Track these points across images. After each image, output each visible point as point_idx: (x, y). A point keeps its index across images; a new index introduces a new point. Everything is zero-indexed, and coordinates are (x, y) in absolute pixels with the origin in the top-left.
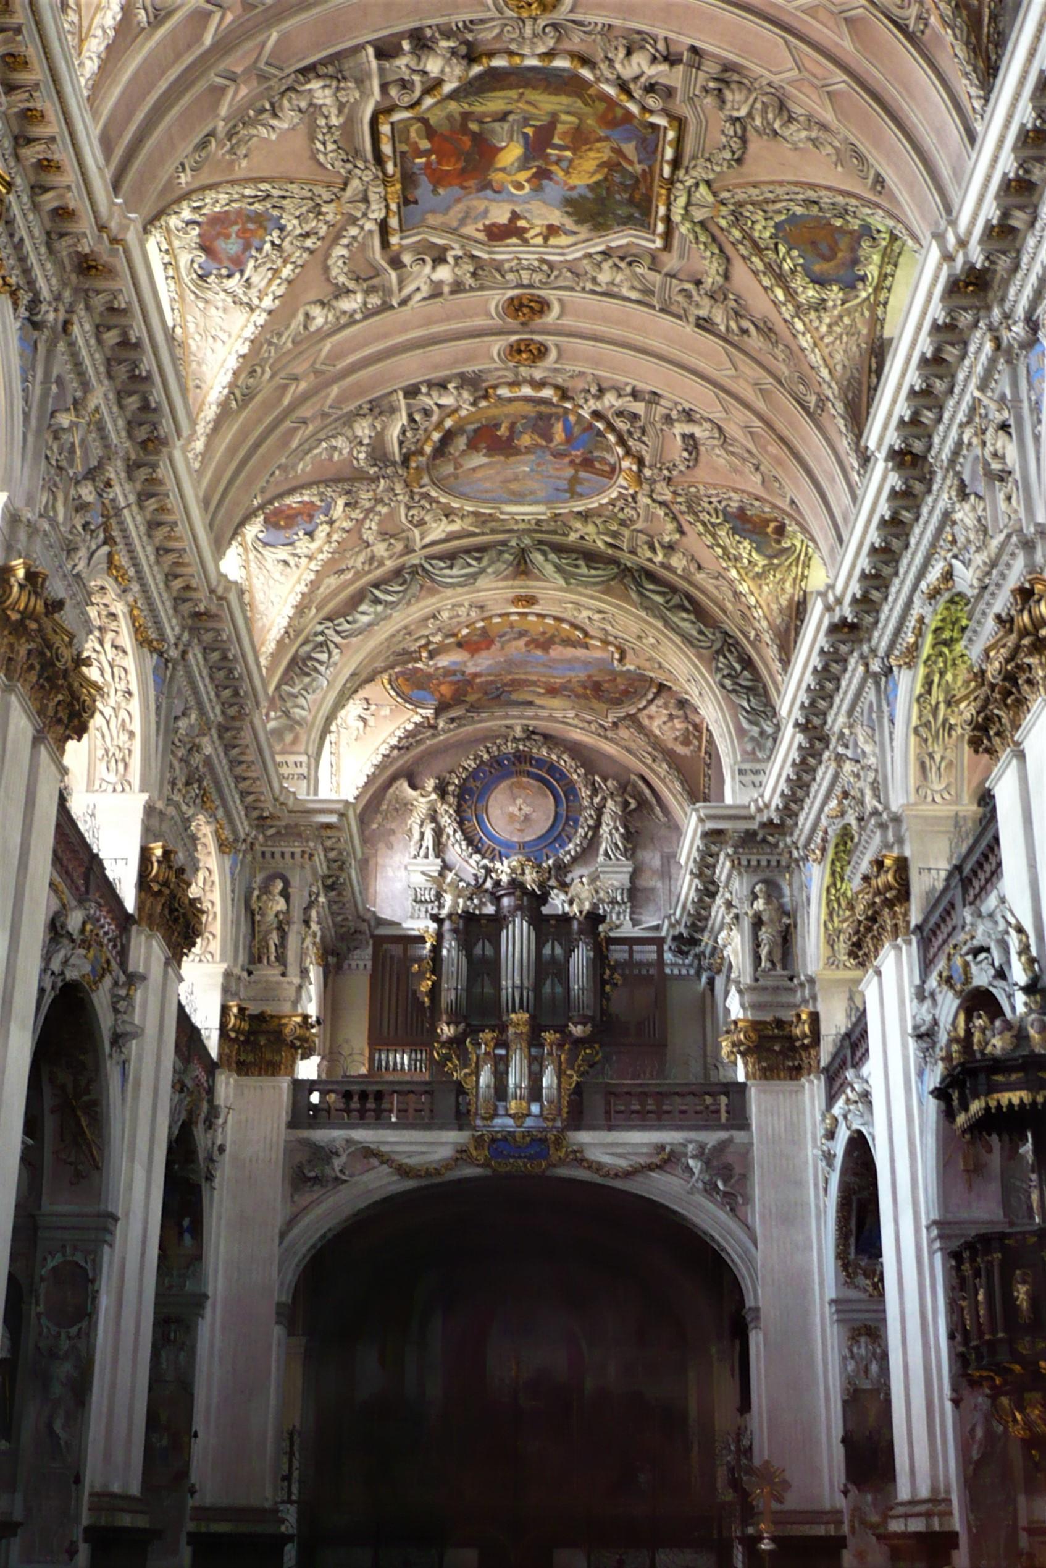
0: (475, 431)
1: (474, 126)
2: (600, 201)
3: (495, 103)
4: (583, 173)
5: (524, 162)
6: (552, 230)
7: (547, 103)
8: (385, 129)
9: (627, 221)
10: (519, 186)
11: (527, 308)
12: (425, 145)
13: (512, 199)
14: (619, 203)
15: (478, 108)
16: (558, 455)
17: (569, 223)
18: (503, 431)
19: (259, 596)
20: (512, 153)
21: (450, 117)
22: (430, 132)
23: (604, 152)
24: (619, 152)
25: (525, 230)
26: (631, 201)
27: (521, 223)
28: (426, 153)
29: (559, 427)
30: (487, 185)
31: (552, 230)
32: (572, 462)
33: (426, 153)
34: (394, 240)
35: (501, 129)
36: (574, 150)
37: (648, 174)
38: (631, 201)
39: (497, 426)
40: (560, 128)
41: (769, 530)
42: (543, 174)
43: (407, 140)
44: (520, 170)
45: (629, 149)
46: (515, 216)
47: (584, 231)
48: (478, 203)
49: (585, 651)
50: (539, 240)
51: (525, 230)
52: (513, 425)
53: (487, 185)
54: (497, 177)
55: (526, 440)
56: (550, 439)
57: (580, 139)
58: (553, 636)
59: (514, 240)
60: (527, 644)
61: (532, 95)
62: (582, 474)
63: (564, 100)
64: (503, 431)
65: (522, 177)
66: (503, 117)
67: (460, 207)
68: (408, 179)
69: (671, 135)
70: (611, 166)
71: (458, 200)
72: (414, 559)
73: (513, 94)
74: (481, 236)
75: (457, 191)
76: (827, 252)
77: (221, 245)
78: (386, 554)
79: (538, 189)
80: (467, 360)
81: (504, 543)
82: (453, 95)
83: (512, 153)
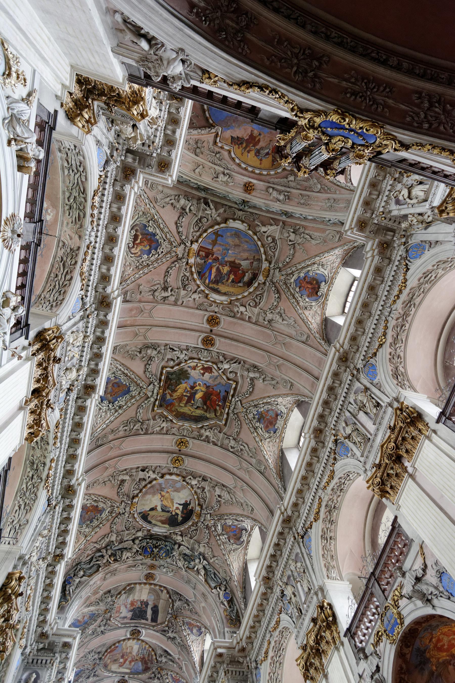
0: (240, 282)
1: (205, 407)
2: (179, 379)
3: (199, 412)
4: (183, 387)
5: (195, 393)
6: (194, 368)
7: (186, 410)
8: (224, 422)
9: (172, 374)
10: (199, 384)
11: (208, 342)
12: (218, 408)
13: (202, 381)
14: (174, 379)
15: (203, 412)
16: (217, 259)
17: (189, 370)
18: (232, 277)
19: (339, 260)
20: (199, 396)
21: (210, 413)
22: (215, 411)
23: (175, 395)
24: (171, 396)
25: (202, 369)
26: (171, 380)
27: (202, 372)
28: (219, 405)
29: (213, 277)
30: (208, 387)
31: (194, 368)
32: (213, 255)
33: (219, 405)
34: (234, 386)
35: (199, 404)
36: (183, 395)
37: (164, 391)
38: (171, 380)
39: (233, 281)
40: (185, 402)
41: (140, 237)
42: (192, 388)
43: (221, 412)
44: (197, 390)
45: (168, 397)
46: (203, 374)
47: (186, 368)
48: (211, 382)
49: (235, 135)
50: (199, 365)
51: (202, 369)
52: (227, 280)
53: (208, 387)
54: (204, 389)
55: (226, 269)
56: (218, 269)
57: (180, 399)
58: (245, 148)
59: (206, 366)
60: (259, 141)
61: (189, 412)
62: (210, 247)
63: (182, 410)
64: (232, 277)
65: (198, 388)
66: (198, 408)
67: (216, 383)
68: (225, 399)
69: (156, 409)
70: (174, 391)
71: (216, 385)
72: (284, 218)
73: (194, 414)
74: (214, 370)
75: (215, 388)
76: (115, 385)
77: (274, 416)
78: (291, 234)
79: (195, 383)
80: (231, 323)
81: (250, 207)
82: (207, 419)
83: (199, 396)
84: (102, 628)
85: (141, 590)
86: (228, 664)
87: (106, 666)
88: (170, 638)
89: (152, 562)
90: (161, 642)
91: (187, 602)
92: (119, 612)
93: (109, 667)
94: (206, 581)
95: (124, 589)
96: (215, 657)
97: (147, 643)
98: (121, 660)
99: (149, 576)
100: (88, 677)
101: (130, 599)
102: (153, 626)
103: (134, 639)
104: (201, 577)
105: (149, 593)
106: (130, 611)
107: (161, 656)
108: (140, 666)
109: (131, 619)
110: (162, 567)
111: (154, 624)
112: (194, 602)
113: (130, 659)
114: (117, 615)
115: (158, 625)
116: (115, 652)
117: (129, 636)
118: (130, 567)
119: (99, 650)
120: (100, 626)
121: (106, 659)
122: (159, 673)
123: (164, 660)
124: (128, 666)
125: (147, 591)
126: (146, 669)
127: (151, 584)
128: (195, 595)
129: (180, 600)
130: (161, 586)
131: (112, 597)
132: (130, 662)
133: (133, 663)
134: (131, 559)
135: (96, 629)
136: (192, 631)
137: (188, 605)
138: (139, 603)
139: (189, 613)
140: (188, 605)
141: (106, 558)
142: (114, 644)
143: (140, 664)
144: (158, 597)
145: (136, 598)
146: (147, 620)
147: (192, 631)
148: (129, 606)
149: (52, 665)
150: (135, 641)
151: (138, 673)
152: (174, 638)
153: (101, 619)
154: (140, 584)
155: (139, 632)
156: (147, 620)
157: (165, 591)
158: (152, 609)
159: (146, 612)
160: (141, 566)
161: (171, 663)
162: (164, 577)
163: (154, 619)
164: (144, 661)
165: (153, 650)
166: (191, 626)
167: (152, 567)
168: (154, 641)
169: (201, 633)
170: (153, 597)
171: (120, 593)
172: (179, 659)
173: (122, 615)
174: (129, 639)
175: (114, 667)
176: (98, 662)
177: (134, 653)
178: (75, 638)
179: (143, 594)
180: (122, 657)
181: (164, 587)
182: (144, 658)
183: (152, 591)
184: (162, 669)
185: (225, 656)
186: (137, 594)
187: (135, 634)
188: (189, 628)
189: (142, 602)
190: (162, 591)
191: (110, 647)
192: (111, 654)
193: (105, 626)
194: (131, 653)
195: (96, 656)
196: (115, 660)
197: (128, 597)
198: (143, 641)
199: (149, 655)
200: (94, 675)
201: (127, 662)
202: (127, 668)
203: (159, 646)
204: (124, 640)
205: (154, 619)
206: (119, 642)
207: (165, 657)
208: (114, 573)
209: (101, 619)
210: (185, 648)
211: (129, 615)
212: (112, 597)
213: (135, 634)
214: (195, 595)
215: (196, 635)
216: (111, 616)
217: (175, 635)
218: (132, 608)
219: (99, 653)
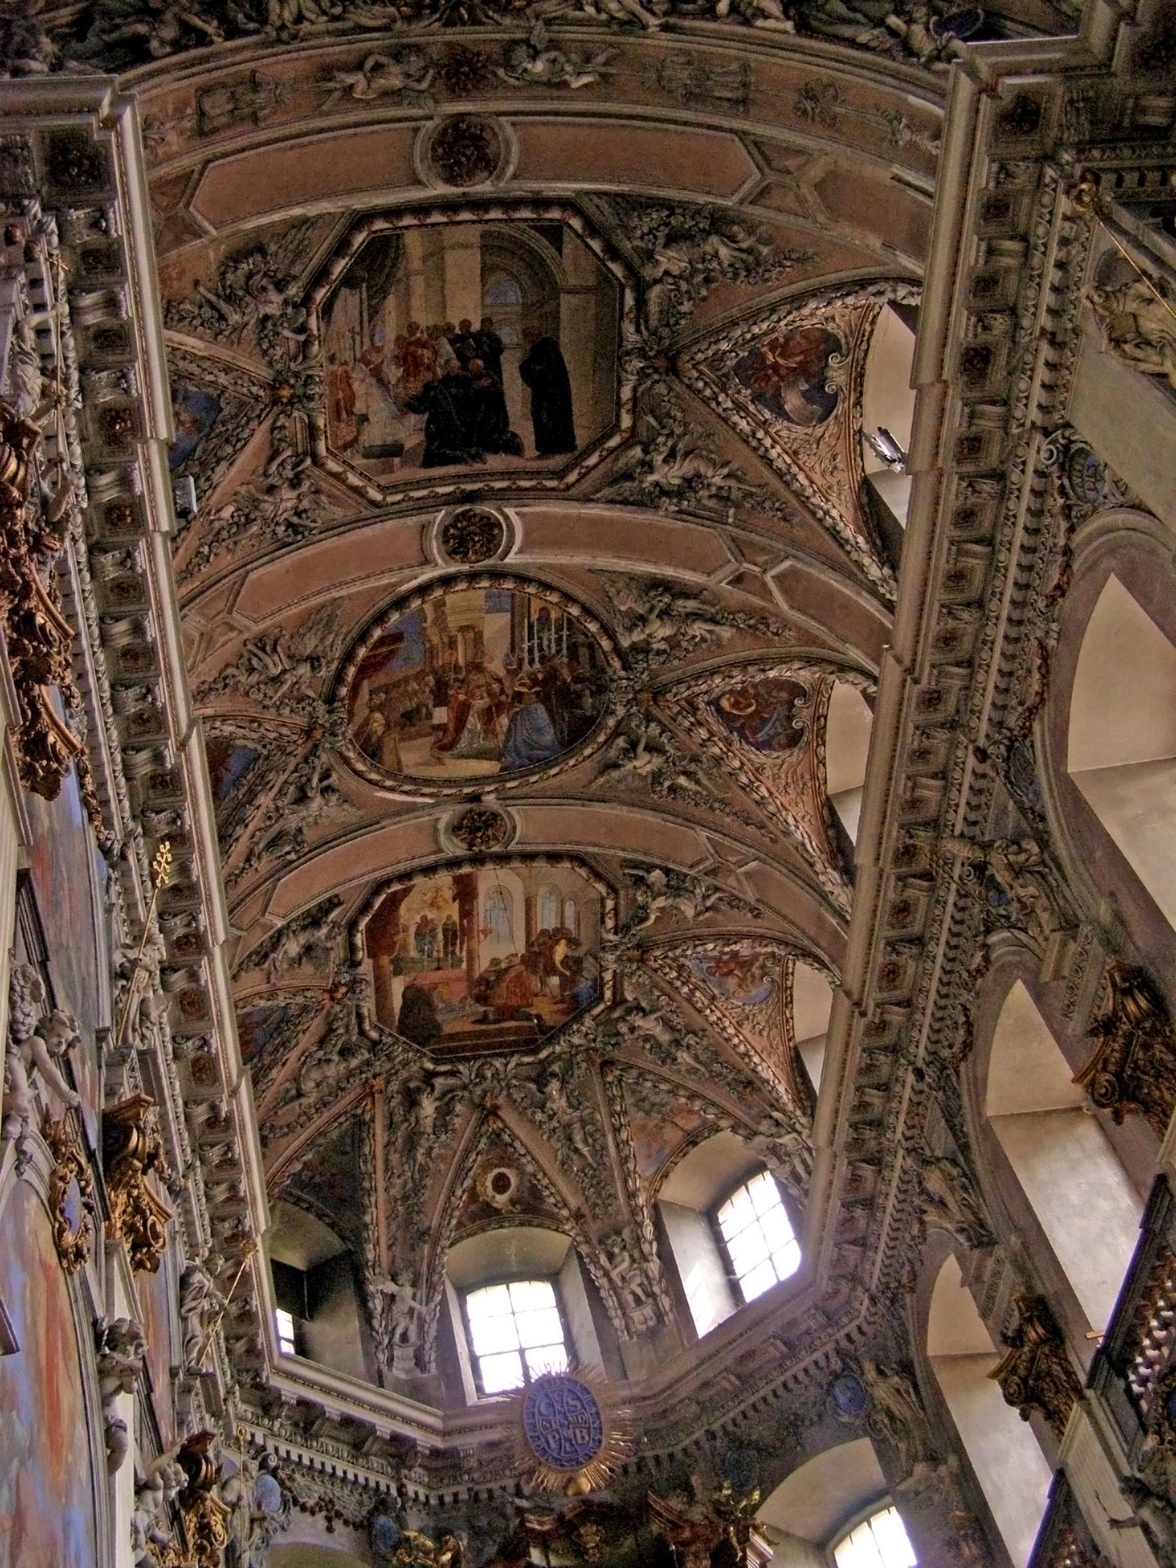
84: (288, 498)
85: (436, 255)
86: (1080, 151)
87: (372, 750)
88: (664, 492)
89: (455, 35)
90: (624, 542)
91: (719, 222)
92: (342, 409)
93: (388, 758)
94: (803, 27)
95: (341, 248)
96: (996, 134)
97: (547, 587)
98: (441, 715)
99: (463, 149)
100: (302, 798)
101: (390, 328)
102: (560, 475)
103: (473, 577)
104: (770, 23)
105: (486, 270)
106: (411, 406)
107: (643, 620)
108: (542, 725)
109: (428, 462)
110: (521, 52)
111: (557, 461)
112: (761, 195)
113: (479, 704)
114: (346, 432)
115: (587, 453)
116: (397, 669)
117: (444, 567)
118: (327, 71)
119: (310, 645)
120: (271, 490)
121: (361, 712)
122: (649, 718)
123: (661, 631)
124: (481, 743)
125: (473, 259)
126: (577, 732)
127: (481, 204)
128: (758, 147)
129: (670, 241)
130: (540, 203)
131: (280, 286)
132: (488, 716)
133: (504, 721)
134: (322, 24)
135: (255, 503)
136: (779, 411)
137: (733, 239)
138: (446, 348)
139: (745, 292)
140: (733, 239)
141: (168, 16)
142: (380, 618)
143: (541, 711)
144: (544, 285)
145: (424, 319)
146: (514, 447)
147: (779, 411)
148: (393, 373)
149: (29, 256)
150: (485, 583)
151: (544, 764)
152: (691, 483)
153: (259, 436)
154: (421, 209)
155: (489, 526)
156: (514, 447)
157: (576, 223)
158: (526, 371)
159: (496, 399)
160: (395, 69)
161: (698, 629)
162: (548, 147)
163: (555, 434)
164: (554, 692)
165: (587, 611)
166: (760, 376)
167: (463, 72)
168: (581, 559)
169: (830, 403)
170: (513, 296)
171: (320, 276)
172: (738, 580)
173: (375, 434)
174: (447, 581)
175: (413, 756)
176: (321, 708)
177: (496, 666)
178: (112, 123)
179: (454, 289)
180: (441, 696)
181: (565, 204)
182: (552, 676)
183: (498, 251)
184: (658, 693)
185: (1055, 111)
186: (418, 284)
187: (472, 536)
188: (757, 398)
189: (462, 340)
190: (554, 233)
191: (363, 637)
192: (381, 678)
193: (295, 483)
194: (477, 667)
195: (304, 670)
196: (409, 717)
197: (375, 312)
198: (522, 579)
199: (573, 651)
200: (326, 791)
201: (473, 722)
202: (479, 755)
203: (613, 576)
204: (423, 590)
205: (555, 434)
206: (400, 603)
207: (665, 614)
208: (246, 101)
209: (259, 436)
210: (761, 504)
211: (411, 432)
212: (280, 286)
213: (472, 536)
214: (758, 147)
215: (805, 421)
216: (312, 430)
217: (687, 467)
218: (415, 387)
219: (314, 661)
